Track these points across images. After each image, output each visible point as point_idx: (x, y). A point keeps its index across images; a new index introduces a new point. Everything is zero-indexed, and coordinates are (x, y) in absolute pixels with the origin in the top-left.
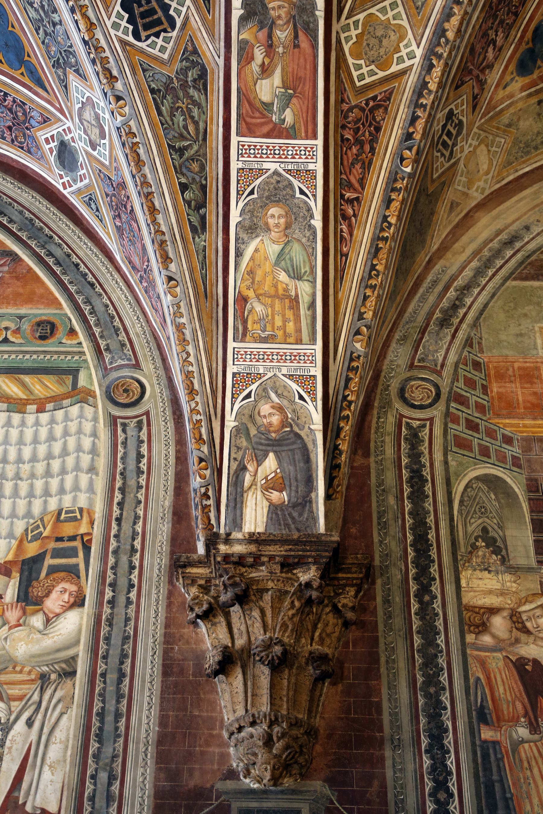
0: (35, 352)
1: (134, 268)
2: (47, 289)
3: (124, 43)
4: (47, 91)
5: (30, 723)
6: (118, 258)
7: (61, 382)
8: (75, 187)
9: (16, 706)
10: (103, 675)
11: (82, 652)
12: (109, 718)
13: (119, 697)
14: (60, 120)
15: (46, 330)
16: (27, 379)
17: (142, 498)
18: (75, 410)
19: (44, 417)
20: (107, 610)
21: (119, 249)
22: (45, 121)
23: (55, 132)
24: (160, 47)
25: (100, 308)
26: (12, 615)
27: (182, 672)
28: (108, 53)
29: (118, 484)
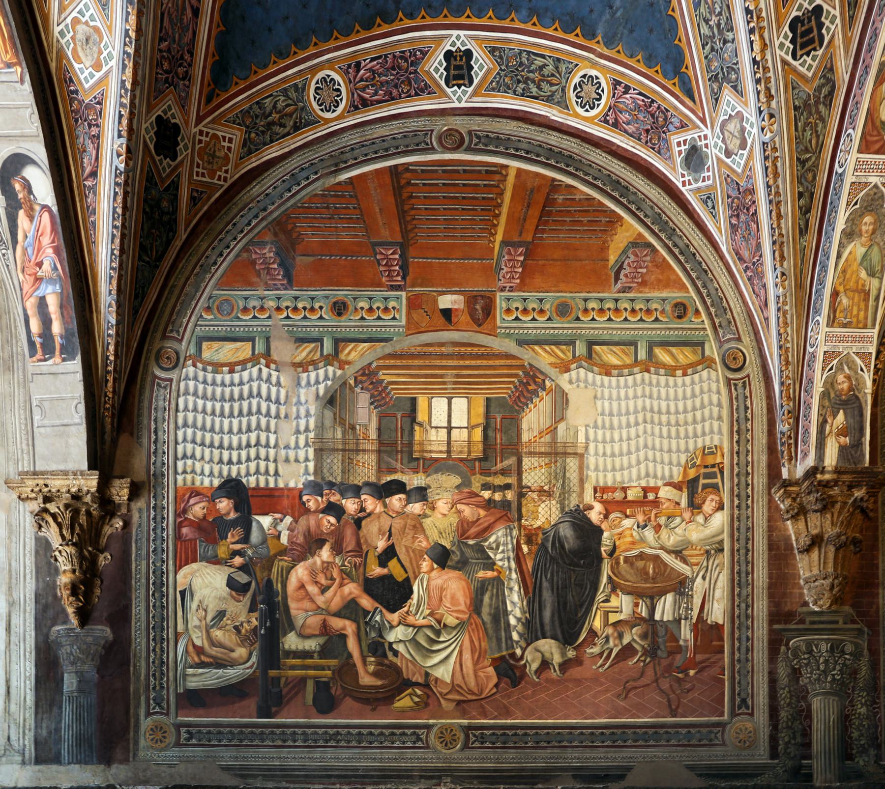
0: (676, 329)
1: (741, 259)
2: (677, 275)
3: (784, 62)
4: (694, 101)
5: (704, 578)
6: (724, 249)
7: (695, 352)
8: (694, 186)
9: (696, 568)
10: (738, 550)
11: (725, 536)
12: (743, 575)
13: (747, 563)
14: (699, 127)
15: (681, 310)
16: (674, 350)
17: (749, 438)
18: (705, 373)
19: (688, 379)
20: (736, 512)
21: (727, 243)
22: (683, 126)
23: (689, 138)
24: (808, 66)
25: (713, 292)
26: (687, 515)
27: (778, 548)
28: (771, 74)
29: (735, 429)
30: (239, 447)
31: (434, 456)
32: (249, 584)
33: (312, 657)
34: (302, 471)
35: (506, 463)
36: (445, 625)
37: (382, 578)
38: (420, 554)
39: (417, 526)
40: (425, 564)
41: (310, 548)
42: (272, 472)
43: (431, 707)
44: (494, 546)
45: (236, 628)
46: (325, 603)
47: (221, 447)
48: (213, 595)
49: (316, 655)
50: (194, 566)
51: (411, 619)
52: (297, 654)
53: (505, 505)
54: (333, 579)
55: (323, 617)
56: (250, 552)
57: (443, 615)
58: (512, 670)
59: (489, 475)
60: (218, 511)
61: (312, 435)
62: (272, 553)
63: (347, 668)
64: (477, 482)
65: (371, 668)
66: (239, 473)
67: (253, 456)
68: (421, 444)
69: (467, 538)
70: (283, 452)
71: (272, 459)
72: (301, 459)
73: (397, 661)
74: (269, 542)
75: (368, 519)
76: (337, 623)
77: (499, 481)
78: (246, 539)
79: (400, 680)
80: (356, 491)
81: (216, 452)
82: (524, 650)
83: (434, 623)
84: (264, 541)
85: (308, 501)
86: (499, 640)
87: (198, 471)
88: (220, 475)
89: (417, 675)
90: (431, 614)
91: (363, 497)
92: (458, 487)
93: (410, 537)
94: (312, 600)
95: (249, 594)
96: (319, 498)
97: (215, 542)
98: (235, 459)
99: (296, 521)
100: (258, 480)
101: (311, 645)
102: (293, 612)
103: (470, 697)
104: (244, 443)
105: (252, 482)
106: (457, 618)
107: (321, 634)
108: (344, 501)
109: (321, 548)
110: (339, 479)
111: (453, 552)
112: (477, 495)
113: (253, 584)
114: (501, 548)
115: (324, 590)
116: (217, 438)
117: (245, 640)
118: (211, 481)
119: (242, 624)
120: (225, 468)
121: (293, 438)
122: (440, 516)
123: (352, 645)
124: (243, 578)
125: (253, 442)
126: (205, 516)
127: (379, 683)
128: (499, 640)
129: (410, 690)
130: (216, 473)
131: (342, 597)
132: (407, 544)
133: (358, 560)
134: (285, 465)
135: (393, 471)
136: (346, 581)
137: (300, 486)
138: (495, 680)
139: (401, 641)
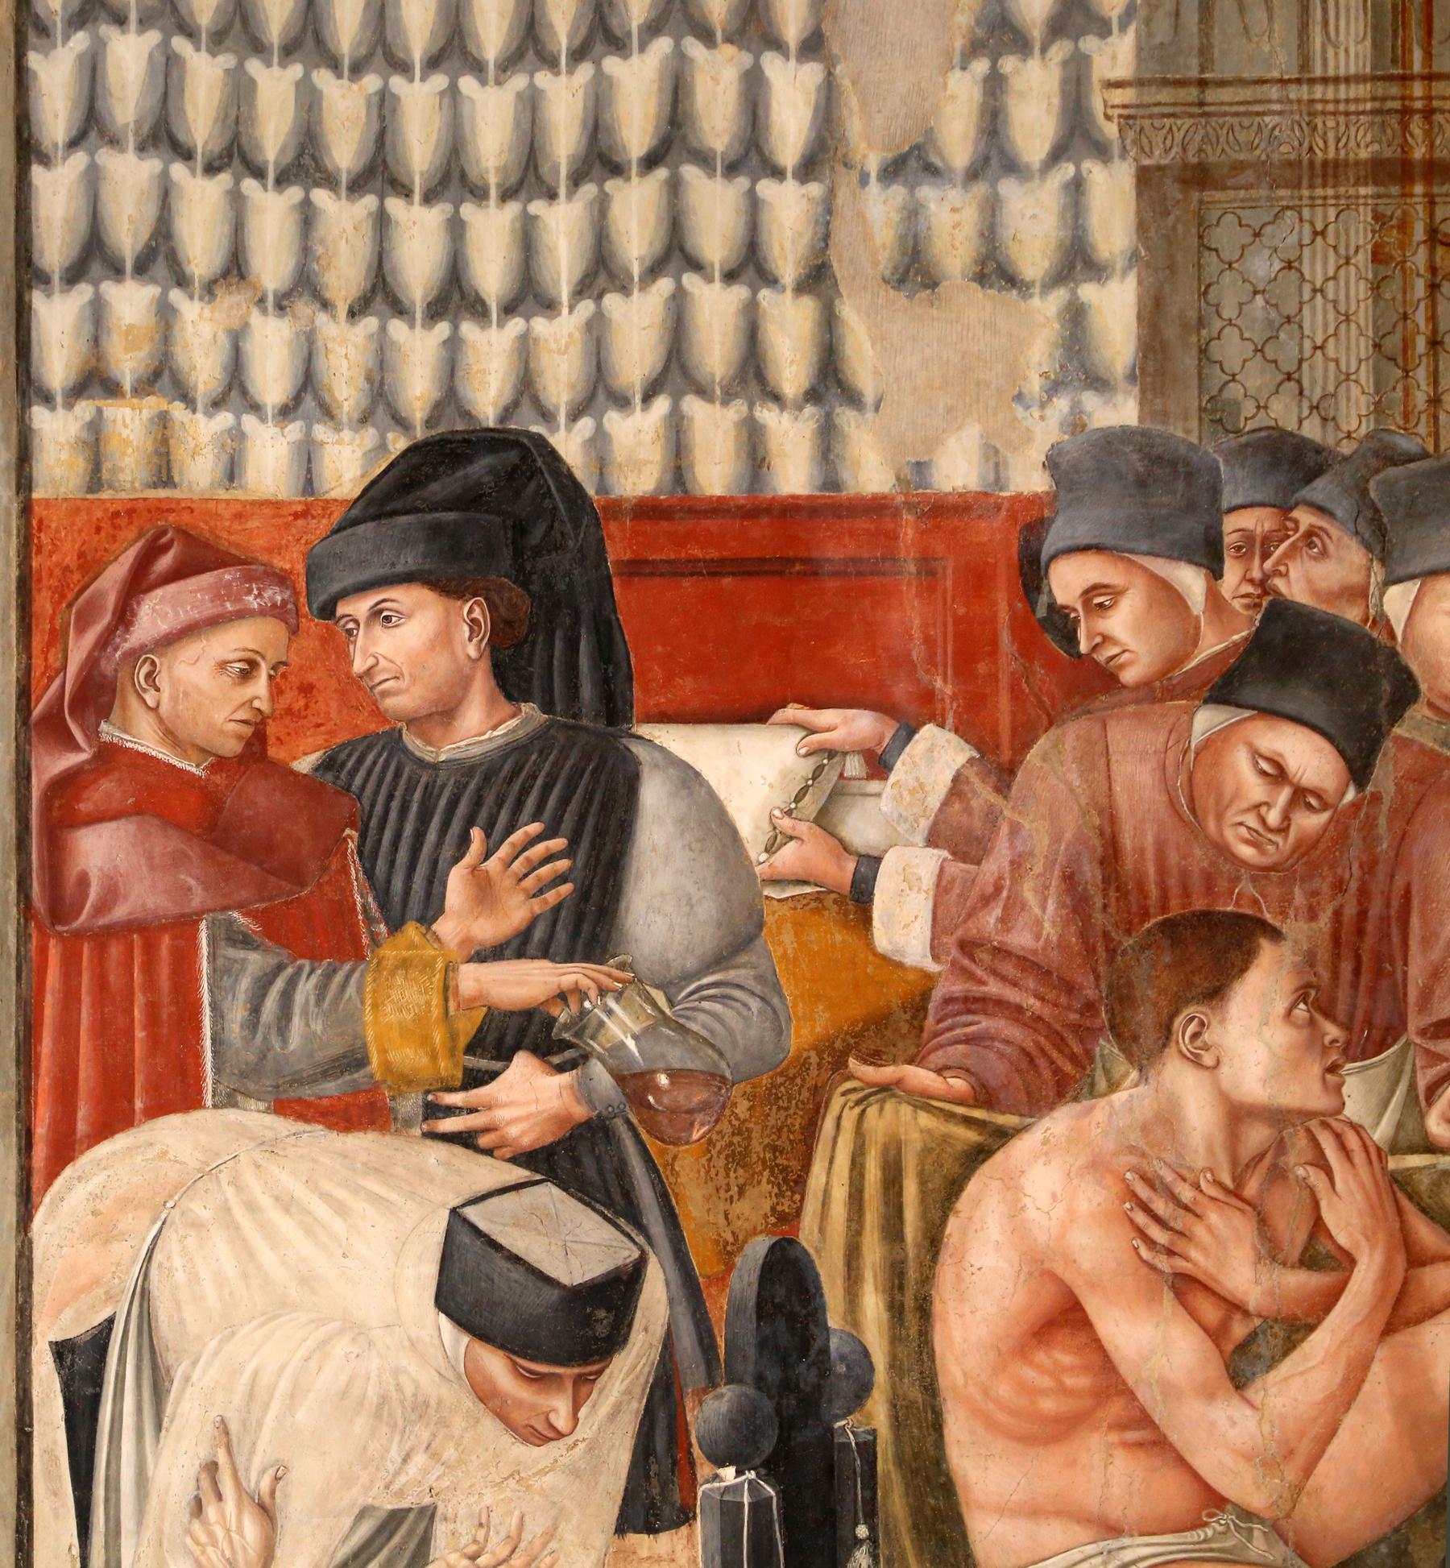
30: (529, 178)
32: (617, 1292)
34: (1040, 354)
41: (1122, 997)
42: (791, 366)
46: (1266, 1463)
47: (380, 173)
48: (328, 1378)
50: (175, 1138)
54: (1323, 1256)
56: (622, 1027)
60: (358, 691)
61: (1115, 56)
62: (799, 1037)
66: (526, 386)
67: (636, 242)
70: (879, 209)
71: (788, 270)
72: (1033, 255)
74: (780, 942)
78: (587, 922)
81: (344, 218)
84: (740, 938)
85: (1098, 599)
87: (204, 367)
88: (381, 400)
94: (1150, 1437)
95: (626, 1376)
96: (1190, 580)
98: (491, 275)
99: (1000, 762)
104: (564, 142)
105: (627, 456)
108: (1397, 601)
109: (1216, 994)
110: (1355, 415)
113: (656, 1296)
115: (1246, 1352)
116: (345, 105)
118: (307, 456)
120: (418, 350)
121: (963, 92)
124: (569, 1242)
125: (635, 133)
130: (345, 386)
131: (1412, 1413)
134: (904, 314)
137: (1029, 478)
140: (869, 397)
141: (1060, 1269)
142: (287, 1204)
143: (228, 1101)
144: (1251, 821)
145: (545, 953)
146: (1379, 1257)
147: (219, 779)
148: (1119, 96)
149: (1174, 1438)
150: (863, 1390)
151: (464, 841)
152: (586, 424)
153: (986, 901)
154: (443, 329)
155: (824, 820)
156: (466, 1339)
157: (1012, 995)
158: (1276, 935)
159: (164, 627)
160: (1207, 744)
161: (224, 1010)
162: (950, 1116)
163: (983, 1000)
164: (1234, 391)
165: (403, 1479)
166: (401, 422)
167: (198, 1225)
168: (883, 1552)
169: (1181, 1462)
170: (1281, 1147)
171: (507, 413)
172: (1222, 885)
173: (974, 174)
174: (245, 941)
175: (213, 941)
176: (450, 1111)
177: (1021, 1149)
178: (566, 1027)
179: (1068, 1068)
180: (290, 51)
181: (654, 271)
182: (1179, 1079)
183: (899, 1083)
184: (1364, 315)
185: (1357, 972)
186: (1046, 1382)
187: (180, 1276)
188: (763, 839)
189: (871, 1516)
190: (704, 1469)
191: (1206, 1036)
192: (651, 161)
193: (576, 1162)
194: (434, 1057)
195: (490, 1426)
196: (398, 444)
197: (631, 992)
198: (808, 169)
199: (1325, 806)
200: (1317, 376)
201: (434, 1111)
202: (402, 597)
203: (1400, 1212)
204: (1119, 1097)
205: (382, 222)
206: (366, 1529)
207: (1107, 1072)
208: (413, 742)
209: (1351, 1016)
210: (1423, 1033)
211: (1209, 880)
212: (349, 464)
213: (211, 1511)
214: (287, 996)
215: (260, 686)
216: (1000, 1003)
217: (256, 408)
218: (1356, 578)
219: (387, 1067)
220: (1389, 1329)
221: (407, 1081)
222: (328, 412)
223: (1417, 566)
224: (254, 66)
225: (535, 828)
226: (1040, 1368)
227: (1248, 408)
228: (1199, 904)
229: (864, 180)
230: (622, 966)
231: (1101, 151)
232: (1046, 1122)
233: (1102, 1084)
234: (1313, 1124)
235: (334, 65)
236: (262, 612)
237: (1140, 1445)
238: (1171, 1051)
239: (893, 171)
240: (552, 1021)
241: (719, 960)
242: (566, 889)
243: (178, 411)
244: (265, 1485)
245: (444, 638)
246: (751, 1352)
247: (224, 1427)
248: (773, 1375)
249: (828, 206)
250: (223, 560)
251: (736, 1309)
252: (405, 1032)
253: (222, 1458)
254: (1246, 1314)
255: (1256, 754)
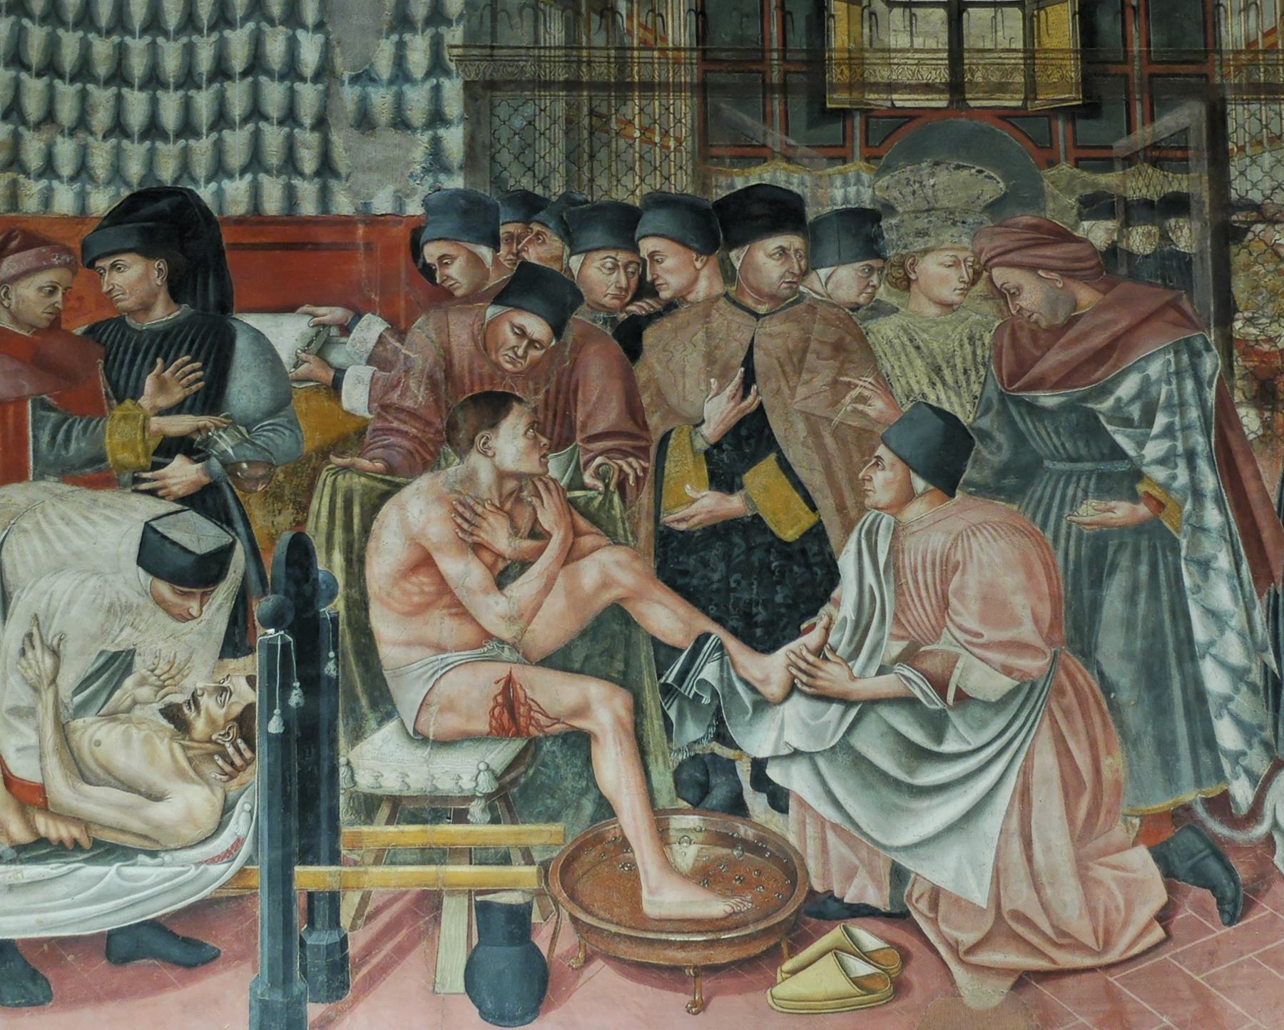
31: (903, 100)
33: (461, 817)
35: (1169, 122)
36: (961, 697)
37: (722, 531)
38: (861, 442)
39: (848, 339)
40: (879, 477)
41: (452, 427)
42: (308, 161)
43: (917, 996)
44: (1135, 411)
45: (173, 714)
49: (476, 808)
51: (834, 676)
52: (402, 808)
53: (1172, 268)
54: (538, 534)
55: (501, 670)
56: (226, 443)
57: (953, 660)
58: (1220, 858)
59: (1106, 165)
60: (107, 299)
61: (454, 35)
62: (308, 447)
63: (594, 859)
64: (1062, 186)
65: (687, 855)
67: (237, 108)
68: (855, 59)
69: (1037, 384)
71: (308, 122)
73: (786, 827)
74: (299, 405)
75: (667, 323)
76: (557, 693)
77: (1142, 184)
78: (210, 397)
79: (800, 896)
80: (623, 224)
82: (1263, 786)
83: (920, 689)
84: (281, 404)
86: (1165, 748)
88: (117, 172)
89: (862, 878)
90: (910, 656)
91: (647, 246)
92: (994, 208)
93: (820, 382)
94: (460, 611)
95: (223, 595)
96: (485, 252)
97: (94, 410)
99: (399, 329)
100: (256, 192)
101: (466, 771)
102: (389, 653)
103: (1066, 959)
105: (234, 195)
106: (1008, 671)
107: (499, 732)
108: (575, 262)
109: (494, 425)
111: (985, 436)
112: (1063, 236)
113: (239, 557)
114: (1161, 420)
115: (503, 577)
117: (206, 757)
119: (194, 701)
120: (136, 154)
122: (932, 311)
123: (613, 768)
124: (198, 534)
125: (238, 62)
126: (55, 324)
127: (717, 907)
128: (1165, 748)
129: (835, 935)
132: (811, 405)
133: (631, 466)
135: (755, 154)
136: (587, 541)
137: (414, 208)
138: (1158, 895)
139: (796, 753)
140: (344, 175)
141: (423, 542)
142: (68, 521)
143: (40, 476)
144: (511, 354)
145: (191, 411)
146: (562, 534)
147: (38, 338)
148: (455, 52)
149: (472, 611)
150: (332, 596)
151: (153, 364)
152: (213, 186)
153: (394, 387)
154: (148, 144)
155: (321, 354)
156: (151, 578)
157: (403, 427)
158: (519, 400)
159: (13, 272)
160: (491, 322)
161: (37, 438)
162: (376, 479)
163: (392, 429)
164: (506, 174)
165: (120, 638)
166: (128, 184)
167: (25, 531)
168: (340, 663)
169: (473, 620)
170: (521, 489)
171: (176, 180)
172: (498, 380)
173: (391, 82)
174: (50, 408)
175: (33, 408)
176: (145, 480)
177: (407, 492)
178: (200, 443)
179: (429, 458)
180: (77, 25)
181: (245, 120)
182: (475, 459)
183: (353, 465)
184: (562, 144)
185: (555, 416)
186: (416, 589)
187: (16, 554)
188: (293, 362)
189: (335, 648)
190: (260, 631)
191: (490, 443)
192: (244, 74)
193: (204, 501)
194: (138, 457)
195: (161, 614)
196: (125, 193)
197: (231, 430)
198: (317, 78)
199: (542, 347)
200: (540, 170)
201: (137, 480)
202: (126, 259)
203: (571, 514)
204: (451, 470)
205: (119, 98)
206: (102, 660)
207: (446, 460)
208: (130, 321)
209: (552, 434)
210: (582, 441)
211: (492, 378)
212: (101, 202)
213: (29, 654)
214: (69, 432)
215: (59, 296)
216: (398, 431)
217: (59, 177)
218: (558, 253)
219: (116, 461)
220: (565, 563)
221: (123, 467)
222: (92, 179)
223: (582, 248)
224: (61, 32)
225: (187, 358)
226: (413, 584)
227: (512, 182)
228: (487, 388)
229: (342, 83)
230: (226, 417)
231: (447, 73)
232: (418, 481)
233: (443, 463)
234: (535, 479)
235: (99, 32)
236: (60, 266)
237: (456, 614)
238: (474, 451)
239: (355, 80)
240: (194, 441)
241: (271, 414)
242: (201, 384)
243: (21, 178)
244: (55, 642)
245: (145, 276)
246: (283, 580)
247: (36, 617)
248: (292, 590)
249: (327, 94)
250: (44, 242)
251: (276, 562)
252: (124, 445)
253: (35, 631)
254: (504, 558)
255: (513, 326)
